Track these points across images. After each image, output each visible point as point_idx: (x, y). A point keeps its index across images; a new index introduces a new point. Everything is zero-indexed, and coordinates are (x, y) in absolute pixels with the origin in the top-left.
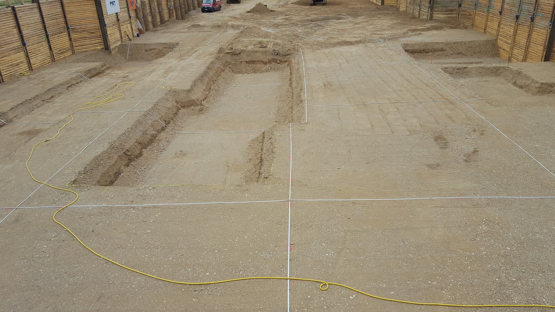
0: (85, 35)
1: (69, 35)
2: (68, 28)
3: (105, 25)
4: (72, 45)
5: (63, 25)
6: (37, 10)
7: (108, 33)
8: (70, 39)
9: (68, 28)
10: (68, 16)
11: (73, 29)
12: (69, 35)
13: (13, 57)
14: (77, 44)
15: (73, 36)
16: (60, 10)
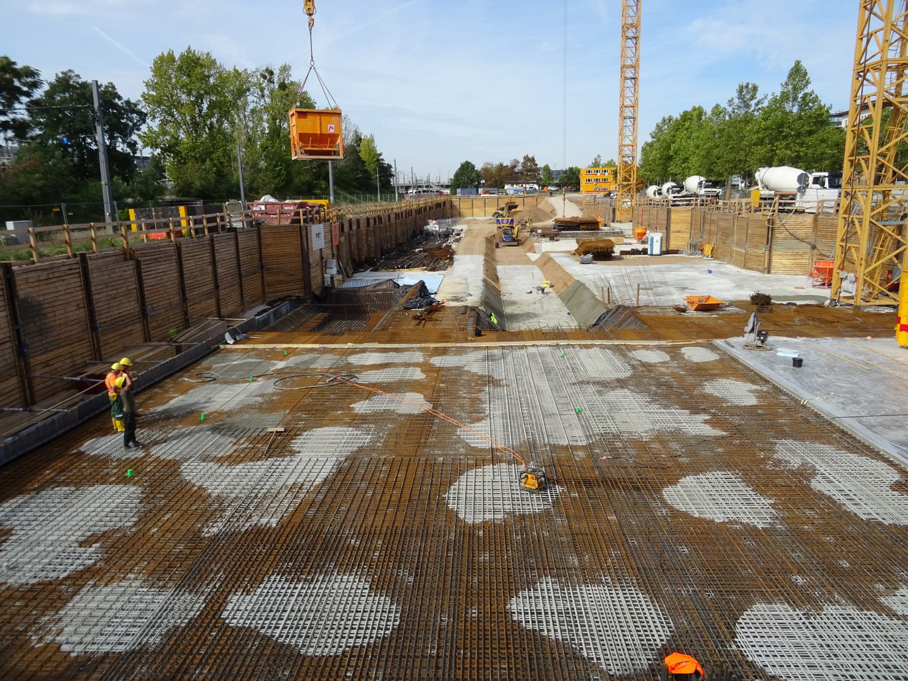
0: (281, 277)
1: (263, 278)
2: (262, 268)
3: (309, 264)
4: (263, 292)
5: (257, 263)
6: (232, 242)
7: (312, 275)
8: (263, 282)
9: (262, 268)
10: (265, 251)
11: (268, 269)
12: (263, 278)
13: (204, 304)
14: (270, 290)
15: (268, 279)
16: (256, 242)
